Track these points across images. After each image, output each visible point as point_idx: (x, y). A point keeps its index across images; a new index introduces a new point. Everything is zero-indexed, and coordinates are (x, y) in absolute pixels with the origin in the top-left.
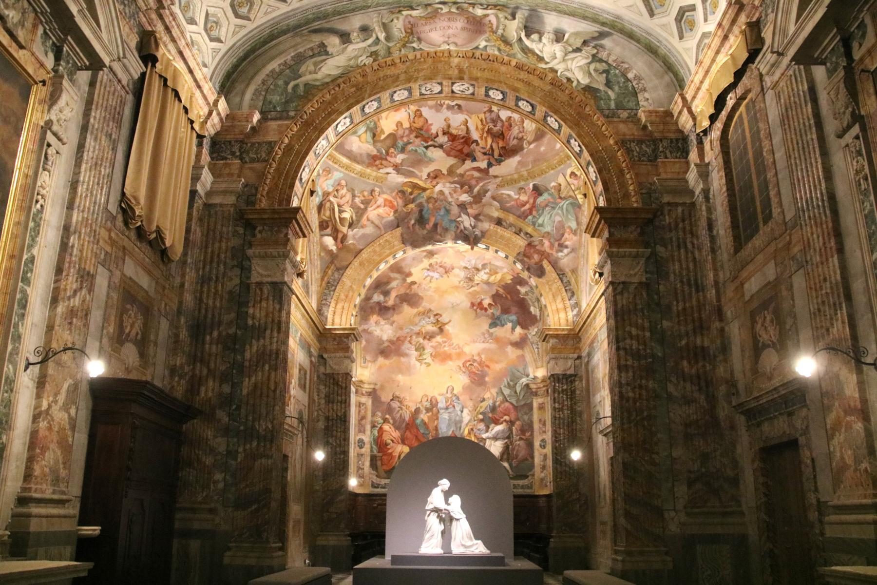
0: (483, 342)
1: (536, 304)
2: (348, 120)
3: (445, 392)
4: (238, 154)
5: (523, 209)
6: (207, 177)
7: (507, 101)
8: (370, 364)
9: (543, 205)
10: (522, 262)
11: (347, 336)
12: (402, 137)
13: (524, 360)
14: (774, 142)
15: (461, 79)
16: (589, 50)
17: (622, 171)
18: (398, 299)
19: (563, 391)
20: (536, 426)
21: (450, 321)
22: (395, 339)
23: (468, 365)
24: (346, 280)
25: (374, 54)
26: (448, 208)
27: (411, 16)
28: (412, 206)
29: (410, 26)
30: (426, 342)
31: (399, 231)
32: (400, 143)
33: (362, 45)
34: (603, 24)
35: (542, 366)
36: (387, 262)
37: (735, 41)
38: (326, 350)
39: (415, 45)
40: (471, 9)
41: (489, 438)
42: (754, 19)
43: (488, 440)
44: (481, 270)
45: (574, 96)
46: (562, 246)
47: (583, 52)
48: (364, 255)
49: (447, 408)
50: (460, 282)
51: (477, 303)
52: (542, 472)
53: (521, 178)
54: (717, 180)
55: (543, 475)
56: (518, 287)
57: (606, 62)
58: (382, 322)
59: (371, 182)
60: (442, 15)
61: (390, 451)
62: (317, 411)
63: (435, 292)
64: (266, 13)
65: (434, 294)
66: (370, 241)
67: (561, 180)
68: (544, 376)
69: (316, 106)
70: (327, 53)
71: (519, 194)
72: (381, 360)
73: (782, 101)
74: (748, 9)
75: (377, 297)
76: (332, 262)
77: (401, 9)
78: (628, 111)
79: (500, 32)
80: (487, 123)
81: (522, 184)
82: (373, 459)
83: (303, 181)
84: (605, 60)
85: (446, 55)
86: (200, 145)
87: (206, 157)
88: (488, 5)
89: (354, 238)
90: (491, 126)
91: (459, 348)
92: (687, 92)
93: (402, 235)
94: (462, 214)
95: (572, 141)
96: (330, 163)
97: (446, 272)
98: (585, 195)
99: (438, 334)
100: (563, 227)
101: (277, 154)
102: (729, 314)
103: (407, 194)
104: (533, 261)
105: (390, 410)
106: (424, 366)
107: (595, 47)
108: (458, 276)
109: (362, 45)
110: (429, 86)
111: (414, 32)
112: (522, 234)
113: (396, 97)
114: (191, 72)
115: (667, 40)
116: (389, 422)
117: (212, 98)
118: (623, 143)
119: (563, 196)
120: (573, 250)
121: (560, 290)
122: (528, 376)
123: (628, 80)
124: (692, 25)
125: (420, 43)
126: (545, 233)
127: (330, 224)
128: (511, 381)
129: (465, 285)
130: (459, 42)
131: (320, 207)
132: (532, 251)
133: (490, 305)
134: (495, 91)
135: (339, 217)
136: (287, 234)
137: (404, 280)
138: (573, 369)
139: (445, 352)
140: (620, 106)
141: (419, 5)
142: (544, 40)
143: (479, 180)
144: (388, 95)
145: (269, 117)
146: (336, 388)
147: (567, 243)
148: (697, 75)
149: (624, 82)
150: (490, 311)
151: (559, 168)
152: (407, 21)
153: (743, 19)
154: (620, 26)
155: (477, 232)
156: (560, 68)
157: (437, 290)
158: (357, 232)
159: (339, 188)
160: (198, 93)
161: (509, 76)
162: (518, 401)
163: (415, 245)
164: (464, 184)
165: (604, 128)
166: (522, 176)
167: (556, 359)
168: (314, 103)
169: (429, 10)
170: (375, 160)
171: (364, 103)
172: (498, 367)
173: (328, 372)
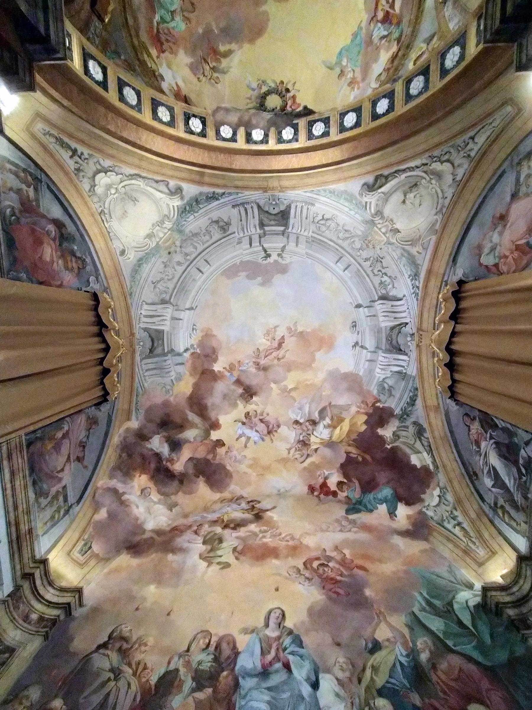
0: (341, 531)
3: (261, 623)
18: (191, 465)
22: (168, 529)
30: (227, 532)
44: (319, 423)
50: (289, 450)
51: (318, 486)
58: (155, 496)
63: (250, 466)
65: (249, 471)
91: (293, 538)
97: (269, 433)
99: (251, 522)
106: (215, 568)
108: (285, 439)
122: (470, 586)
133: (340, 484)
137: (207, 434)
139: (265, 546)
150: (342, 495)
157: (255, 464)
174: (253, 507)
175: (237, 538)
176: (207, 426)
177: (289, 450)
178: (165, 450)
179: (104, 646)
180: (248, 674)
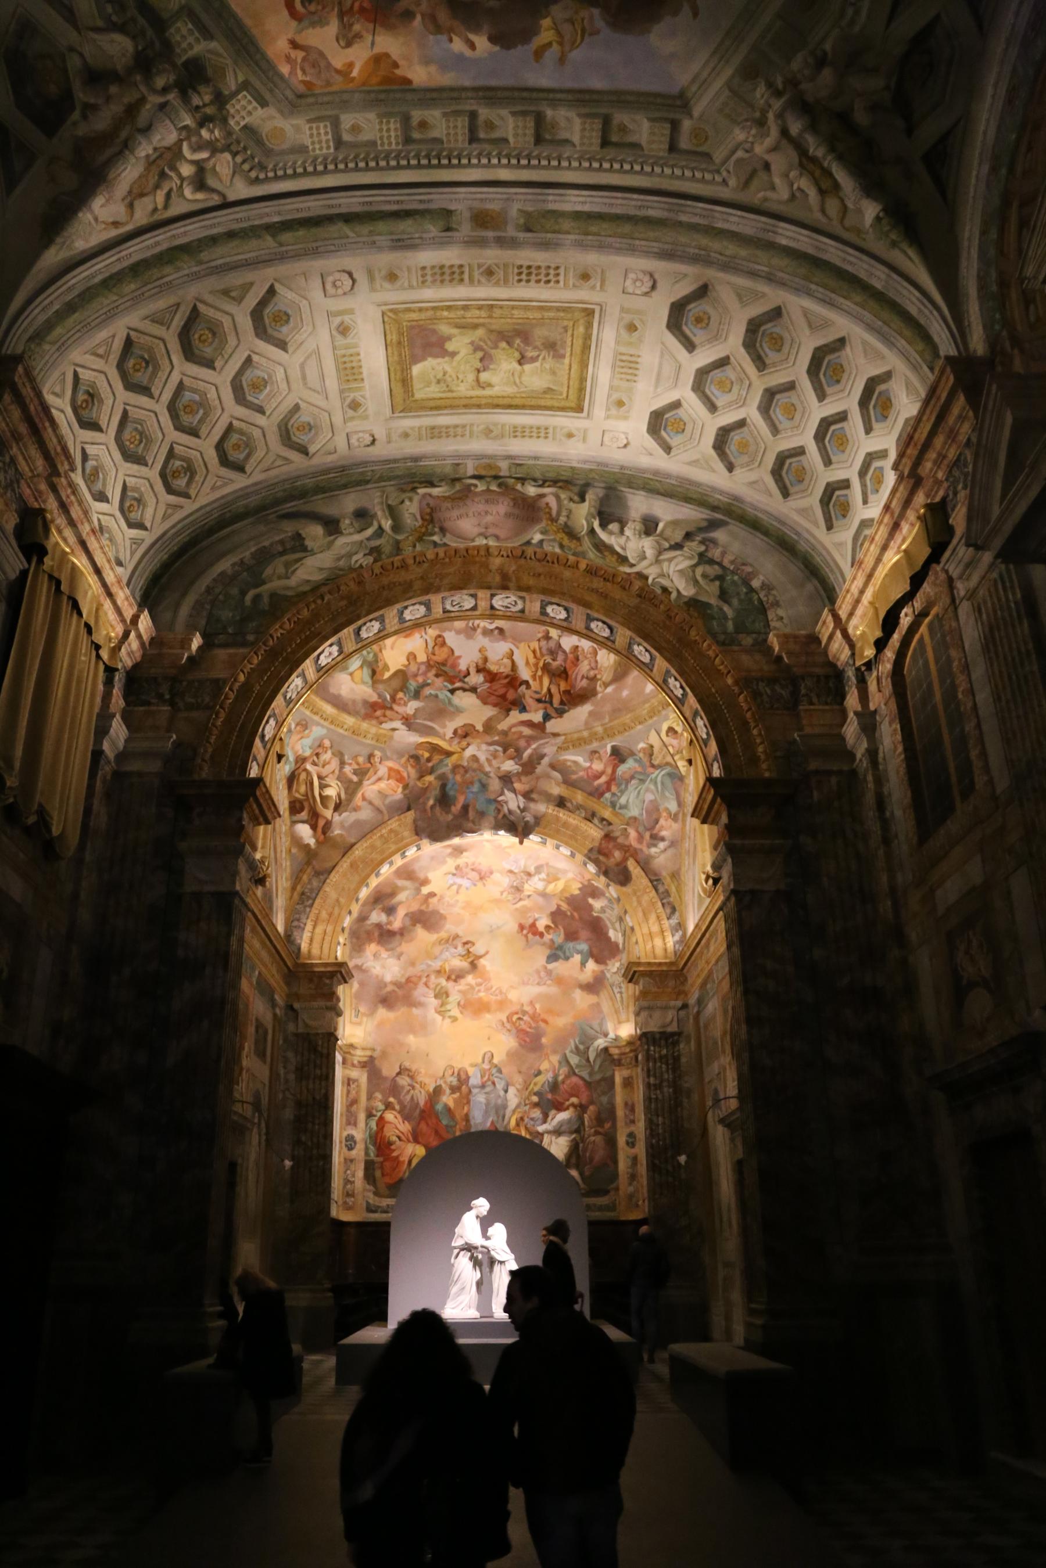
0: (538, 984)
1: (617, 925)
2: (335, 648)
3: (480, 1060)
4: (167, 697)
5: (597, 783)
6: (118, 730)
7: (574, 622)
8: (365, 1019)
9: (627, 776)
10: (596, 862)
11: (332, 975)
12: (416, 676)
13: (601, 1012)
14: (974, 677)
15: (505, 588)
16: (694, 547)
17: (745, 723)
19: (661, 1057)
20: (620, 1113)
21: (487, 953)
22: (403, 980)
23: (515, 1017)
24: (330, 890)
25: (375, 551)
26: (484, 781)
27: (430, 495)
28: (430, 778)
29: (428, 510)
30: (450, 985)
31: (410, 815)
32: (413, 685)
33: (357, 537)
34: (714, 508)
35: (628, 1020)
36: (391, 863)
37: (910, 532)
38: (298, 997)
39: (436, 538)
40: (519, 487)
41: (549, 1132)
42: (937, 499)
43: (546, 1136)
44: (534, 875)
45: (673, 614)
46: (656, 838)
47: (685, 549)
48: (358, 852)
49: (483, 1086)
51: (527, 925)
52: (630, 1184)
53: (594, 736)
54: (889, 734)
55: (631, 1189)
56: (590, 900)
57: (720, 564)
58: (384, 954)
59: (368, 741)
60: (477, 494)
61: (395, 1154)
62: (284, 1092)
63: (463, 908)
64: (213, 488)
66: (366, 831)
67: (654, 739)
68: (631, 1036)
69: (287, 626)
70: (305, 549)
71: (591, 760)
72: (382, 1012)
73: (984, 616)
74: (928, 483)
75: (377, 917)
76: (308, 863)
77: (416, 485)
78: (754, 635)
79: (562, 519)
80: (542, 655)
81: (595, 745)
82: (369, 1166)
83: (267, 739)
84: (718, 560)
85: (482, 553)
86: (109, 682)
87: (118, 701)
88: (545, 481)
89: (342, 827)
90: (548, 659)
91: (501, 992)
92: (840, 607)
93: (415, 821)
94: (506, 791)
95: (671, 681)
96: (308, 713)
97: (481, 878)
98: (690, 762)
99: (468, 973)
100: (658, 810)
101: (226, 698)
102: (913, 937)
103: (423, 761)
104: (612, 860)
105: (394, 1089)
106: (448, 1021)
107: (703, 542)
109: (357, 537)
110: (457, 598)
111: (436, 520)
112: (596, 821)
113: (407, 615)
114: (98, 571)
115: (808, 531)
116: (394, 1109)
117: (129, 613)
118: (746, 682)
119: (656, 763)
120: (673, 844)
121: (653, 904)
122: (606, 1035)
123: (752, 590)
124: (845, 509)
125: (444, 536)
126: (630, 818)
127: (306, 804)
128: (582, 1043)
129: (510, 897)
130: (502, 534)
131: (291, 779)
132: (611, 845)
133: (548, 927)
134: (555, 607)
135: (320, 794)
136: (240, 819)
138: (675, 1024)
139: (480, 999)
140: (741, 627)
141: (442, 480)
142: (628, 532)
143: (530, 739)
144: (395, 611)
145: (216, 641)
146: (313, 1056)
147: (663, 833)
148: (856, 582)
149: (746, 593)
150: (548, 937)
151: (650, 722)
152: (424, 503)
153: (920, 499)
154: (740, 512)
155: (529, 818)
156: (652, 573)
157: (468, 905)
158: (347, 817)
159: (320, 750)
160: (107, 605)
161: (575, 584)
162: (591, 1074)
163: (436, 836)
164: (508, 746)
165: (717, 661)
166: (596, 734)
167: (649, 1008)
168: (284, 623)
169: (458, 486)
170: (375, 710)
171: (360, 622)
172: (561, 1022)
173: (301, 1030)
174: (469, 952)
175: (460, 991)
176: (417, 885)
177: (502, 893)
178: (383, 918)
179: (399, 1074)
180: (475, 1087)
